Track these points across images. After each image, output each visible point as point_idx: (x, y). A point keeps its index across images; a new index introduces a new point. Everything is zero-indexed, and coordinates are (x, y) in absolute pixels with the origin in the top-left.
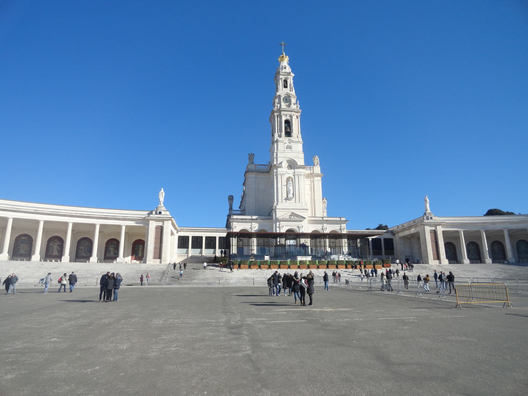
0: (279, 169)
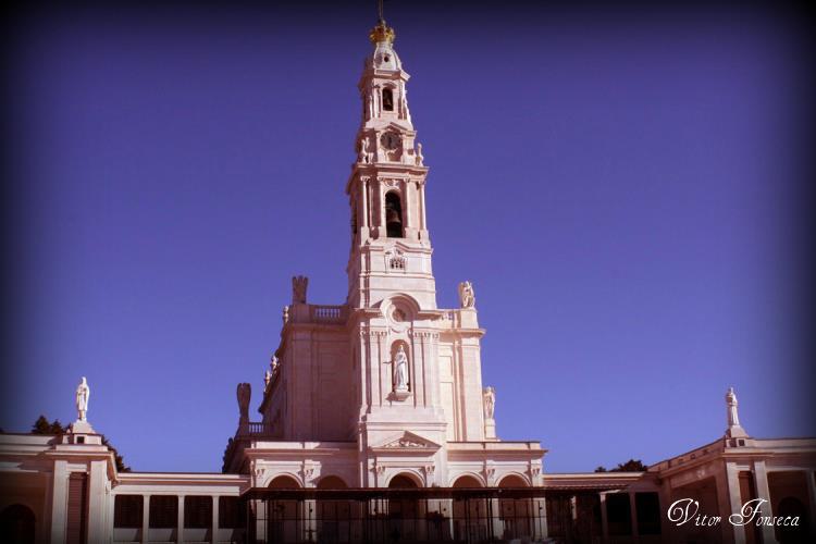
0: (373, 322)
